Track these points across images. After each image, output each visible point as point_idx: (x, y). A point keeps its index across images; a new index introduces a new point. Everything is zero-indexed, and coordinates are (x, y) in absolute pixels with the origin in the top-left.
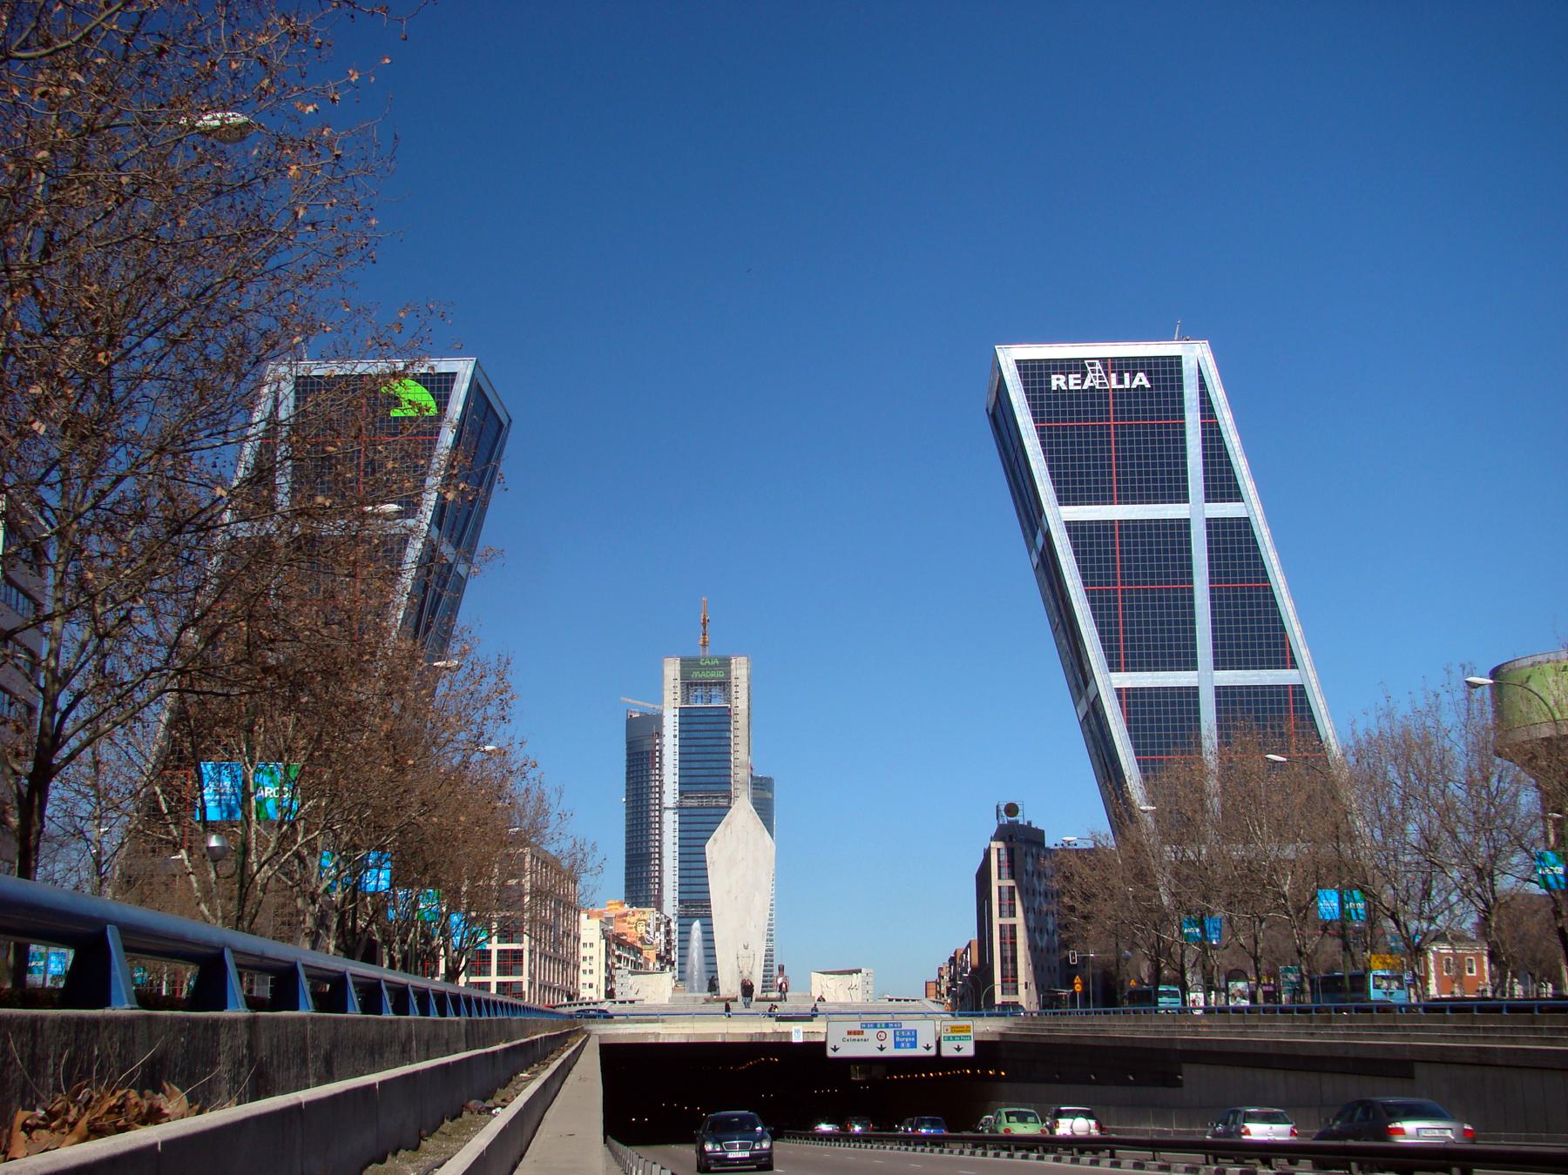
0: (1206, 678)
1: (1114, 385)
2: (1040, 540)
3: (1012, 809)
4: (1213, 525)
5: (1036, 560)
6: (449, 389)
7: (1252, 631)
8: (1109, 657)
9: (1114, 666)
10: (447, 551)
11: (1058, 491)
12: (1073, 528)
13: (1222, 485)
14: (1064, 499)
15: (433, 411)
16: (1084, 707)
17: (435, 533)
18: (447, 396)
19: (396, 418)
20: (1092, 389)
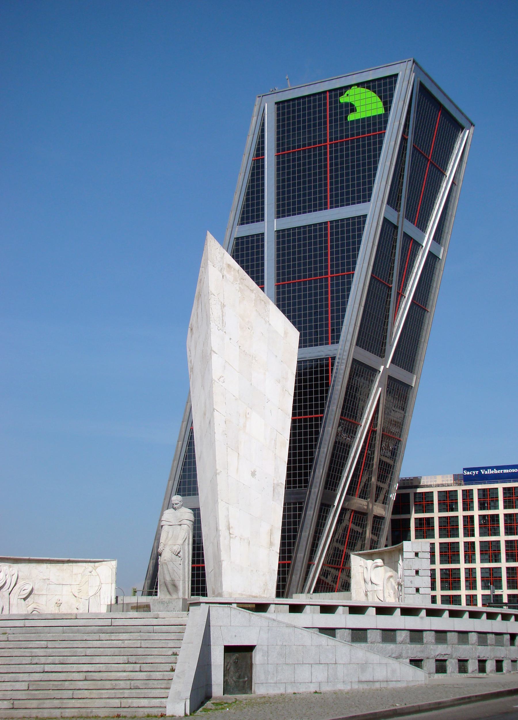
6: (392, 90)
10: (408, 228)
15: (381, 111)
18: (392, 96)
19: (352, 122)
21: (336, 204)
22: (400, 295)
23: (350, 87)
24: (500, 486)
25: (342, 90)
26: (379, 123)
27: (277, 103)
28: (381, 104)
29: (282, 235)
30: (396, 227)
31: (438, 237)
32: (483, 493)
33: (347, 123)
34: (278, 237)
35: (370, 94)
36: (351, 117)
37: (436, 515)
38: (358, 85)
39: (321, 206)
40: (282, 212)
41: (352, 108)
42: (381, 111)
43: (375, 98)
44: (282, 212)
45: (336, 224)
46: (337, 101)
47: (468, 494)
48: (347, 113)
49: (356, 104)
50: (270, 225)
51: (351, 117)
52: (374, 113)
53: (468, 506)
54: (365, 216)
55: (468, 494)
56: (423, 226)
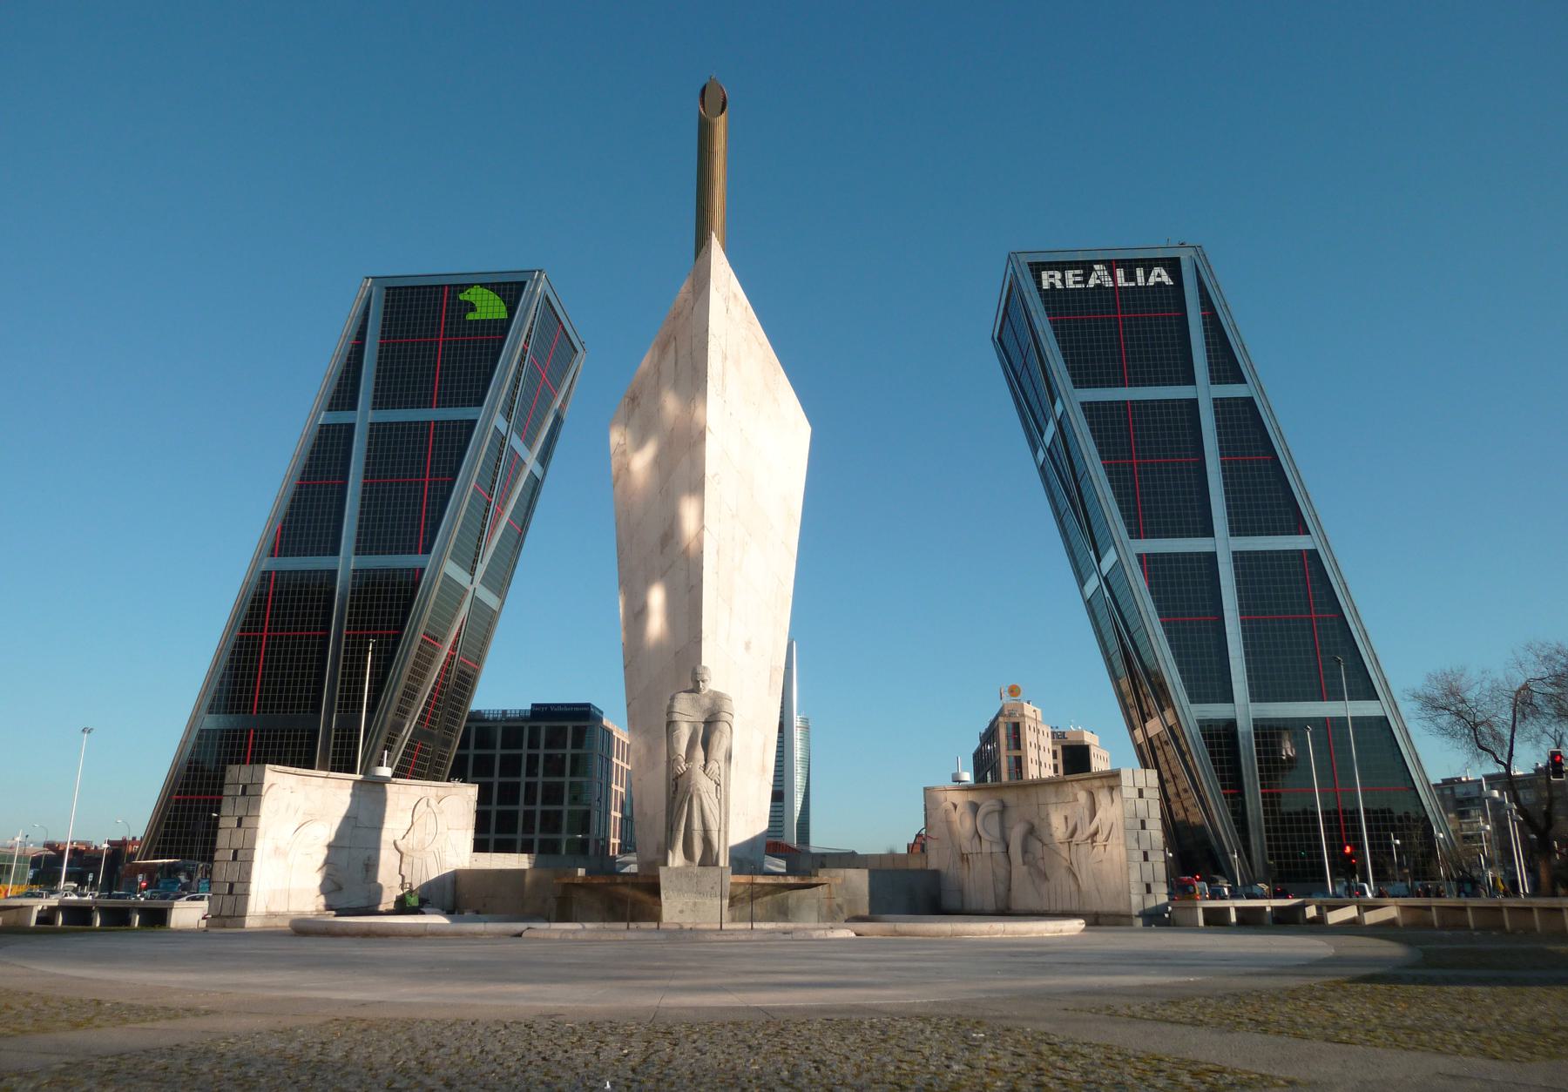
0: (1224, 544)
1: (1121, 282)
2: (1051, 429)
3: (1014, 691)
4: (1220, 405)
5: (1041, 455)
7: (1268, 495)
8: (1128, 525)
9: (1135, 533)
10: (516, 442)
11: (1073, 376)
12: (1089, 408)
13: (1227, 366)
14: (1079, 383)
15: (504, 315)
16: (1093, 583)
17: (499, 422)
20: (1099, 286)
21: (443, 404)
22: (498, 515)
23: (472, 285)
24: (570, 726)
25: (463, 287)
26: (503, 327)
27: (388, 288)
28: (504, 308)
29: (375, 428)
30: (504, 438)
31: (544, 458)
32: (550, 731)
33: (465, 322)
34: (371, 430)
35: (492, 295)
36: (470, 316)
37: (498, 752)
38: (482, 285)
39: (427, 404)
40: (378, 404)
41: (471, 307)
42: (504, 315)
43: (498, 301)
44: (378, 404)
45: (440, 424)
46: (456, 298)
47: (534, 732)
48: (466, 311)
49: (477, 304)
50: (363, 416)
51: (470, 316)
52: (496, 317)
53: (533, 744)
54: (475, 421)
55: (534, 732)
56: (529, 444)
